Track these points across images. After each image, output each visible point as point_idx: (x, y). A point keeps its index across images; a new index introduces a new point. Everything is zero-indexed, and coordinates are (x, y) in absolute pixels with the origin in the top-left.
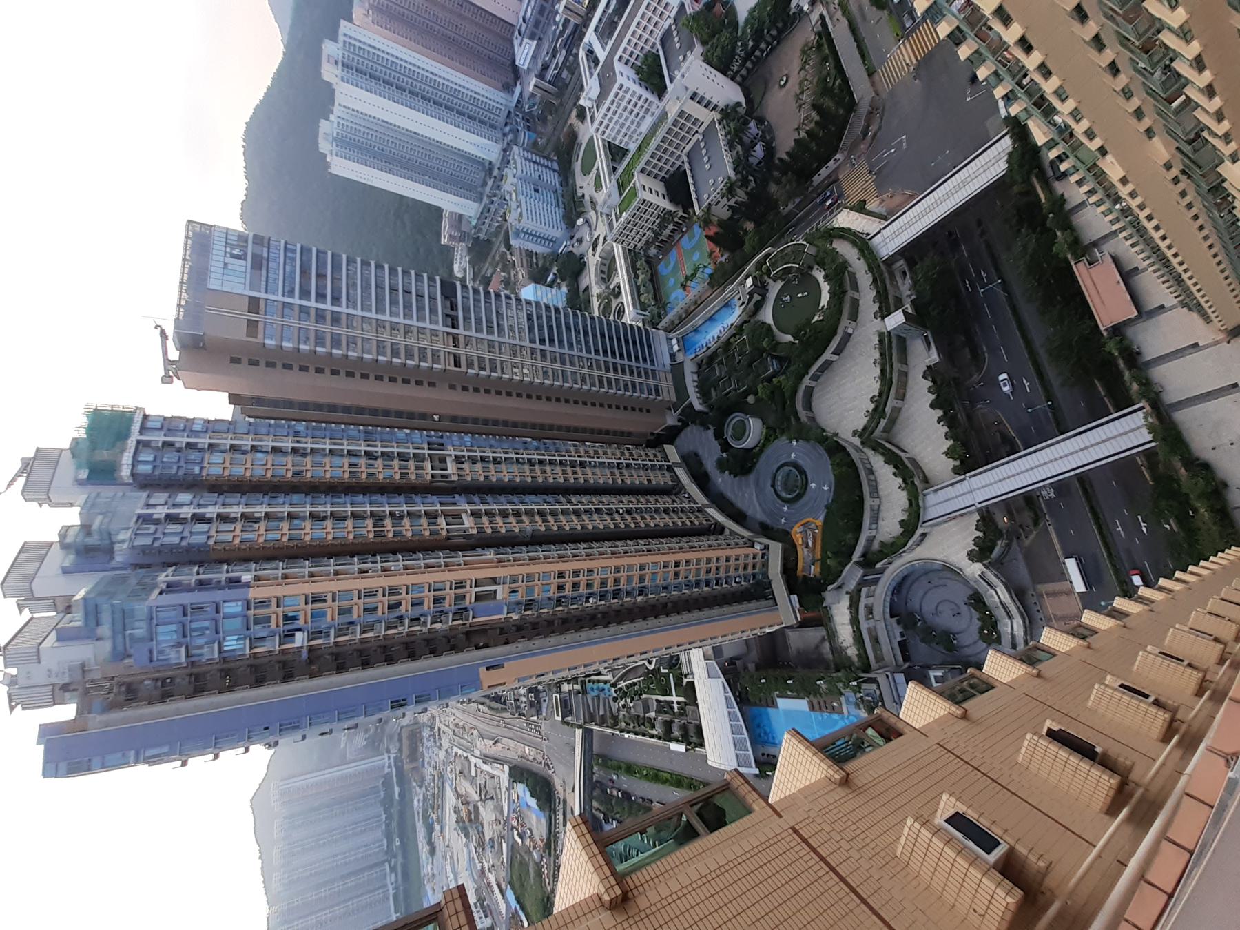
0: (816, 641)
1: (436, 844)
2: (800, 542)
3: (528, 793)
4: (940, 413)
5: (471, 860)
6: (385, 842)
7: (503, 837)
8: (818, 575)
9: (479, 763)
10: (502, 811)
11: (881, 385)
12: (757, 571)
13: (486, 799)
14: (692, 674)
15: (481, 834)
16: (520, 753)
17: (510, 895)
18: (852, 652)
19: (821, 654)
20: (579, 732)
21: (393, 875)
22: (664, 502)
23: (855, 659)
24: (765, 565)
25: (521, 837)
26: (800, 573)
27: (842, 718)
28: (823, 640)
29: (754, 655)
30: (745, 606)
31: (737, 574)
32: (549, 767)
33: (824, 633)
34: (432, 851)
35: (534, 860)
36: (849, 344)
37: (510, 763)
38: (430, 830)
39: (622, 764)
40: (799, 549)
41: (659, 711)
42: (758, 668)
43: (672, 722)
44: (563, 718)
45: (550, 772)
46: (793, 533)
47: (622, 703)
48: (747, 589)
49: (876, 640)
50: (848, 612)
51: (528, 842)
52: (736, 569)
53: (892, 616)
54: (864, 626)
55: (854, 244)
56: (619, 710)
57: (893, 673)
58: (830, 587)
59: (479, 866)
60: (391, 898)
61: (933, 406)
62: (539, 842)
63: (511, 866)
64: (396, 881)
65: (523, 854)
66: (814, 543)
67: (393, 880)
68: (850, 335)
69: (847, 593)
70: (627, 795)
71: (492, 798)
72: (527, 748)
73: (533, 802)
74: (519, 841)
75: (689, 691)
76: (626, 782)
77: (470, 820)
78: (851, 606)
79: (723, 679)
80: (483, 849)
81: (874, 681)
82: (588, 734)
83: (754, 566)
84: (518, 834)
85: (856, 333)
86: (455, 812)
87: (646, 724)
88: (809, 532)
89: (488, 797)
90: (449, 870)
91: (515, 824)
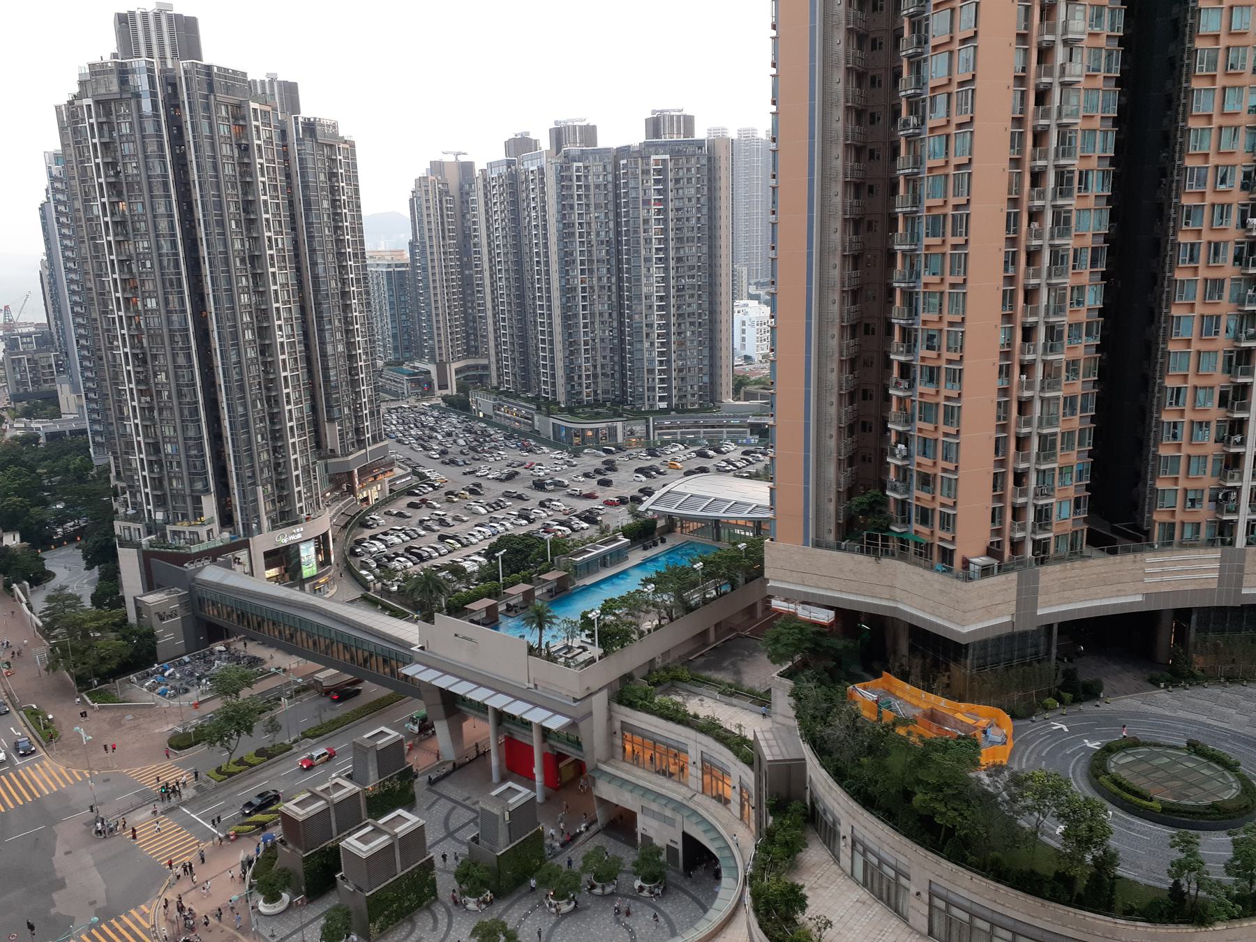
19: (724, 669)
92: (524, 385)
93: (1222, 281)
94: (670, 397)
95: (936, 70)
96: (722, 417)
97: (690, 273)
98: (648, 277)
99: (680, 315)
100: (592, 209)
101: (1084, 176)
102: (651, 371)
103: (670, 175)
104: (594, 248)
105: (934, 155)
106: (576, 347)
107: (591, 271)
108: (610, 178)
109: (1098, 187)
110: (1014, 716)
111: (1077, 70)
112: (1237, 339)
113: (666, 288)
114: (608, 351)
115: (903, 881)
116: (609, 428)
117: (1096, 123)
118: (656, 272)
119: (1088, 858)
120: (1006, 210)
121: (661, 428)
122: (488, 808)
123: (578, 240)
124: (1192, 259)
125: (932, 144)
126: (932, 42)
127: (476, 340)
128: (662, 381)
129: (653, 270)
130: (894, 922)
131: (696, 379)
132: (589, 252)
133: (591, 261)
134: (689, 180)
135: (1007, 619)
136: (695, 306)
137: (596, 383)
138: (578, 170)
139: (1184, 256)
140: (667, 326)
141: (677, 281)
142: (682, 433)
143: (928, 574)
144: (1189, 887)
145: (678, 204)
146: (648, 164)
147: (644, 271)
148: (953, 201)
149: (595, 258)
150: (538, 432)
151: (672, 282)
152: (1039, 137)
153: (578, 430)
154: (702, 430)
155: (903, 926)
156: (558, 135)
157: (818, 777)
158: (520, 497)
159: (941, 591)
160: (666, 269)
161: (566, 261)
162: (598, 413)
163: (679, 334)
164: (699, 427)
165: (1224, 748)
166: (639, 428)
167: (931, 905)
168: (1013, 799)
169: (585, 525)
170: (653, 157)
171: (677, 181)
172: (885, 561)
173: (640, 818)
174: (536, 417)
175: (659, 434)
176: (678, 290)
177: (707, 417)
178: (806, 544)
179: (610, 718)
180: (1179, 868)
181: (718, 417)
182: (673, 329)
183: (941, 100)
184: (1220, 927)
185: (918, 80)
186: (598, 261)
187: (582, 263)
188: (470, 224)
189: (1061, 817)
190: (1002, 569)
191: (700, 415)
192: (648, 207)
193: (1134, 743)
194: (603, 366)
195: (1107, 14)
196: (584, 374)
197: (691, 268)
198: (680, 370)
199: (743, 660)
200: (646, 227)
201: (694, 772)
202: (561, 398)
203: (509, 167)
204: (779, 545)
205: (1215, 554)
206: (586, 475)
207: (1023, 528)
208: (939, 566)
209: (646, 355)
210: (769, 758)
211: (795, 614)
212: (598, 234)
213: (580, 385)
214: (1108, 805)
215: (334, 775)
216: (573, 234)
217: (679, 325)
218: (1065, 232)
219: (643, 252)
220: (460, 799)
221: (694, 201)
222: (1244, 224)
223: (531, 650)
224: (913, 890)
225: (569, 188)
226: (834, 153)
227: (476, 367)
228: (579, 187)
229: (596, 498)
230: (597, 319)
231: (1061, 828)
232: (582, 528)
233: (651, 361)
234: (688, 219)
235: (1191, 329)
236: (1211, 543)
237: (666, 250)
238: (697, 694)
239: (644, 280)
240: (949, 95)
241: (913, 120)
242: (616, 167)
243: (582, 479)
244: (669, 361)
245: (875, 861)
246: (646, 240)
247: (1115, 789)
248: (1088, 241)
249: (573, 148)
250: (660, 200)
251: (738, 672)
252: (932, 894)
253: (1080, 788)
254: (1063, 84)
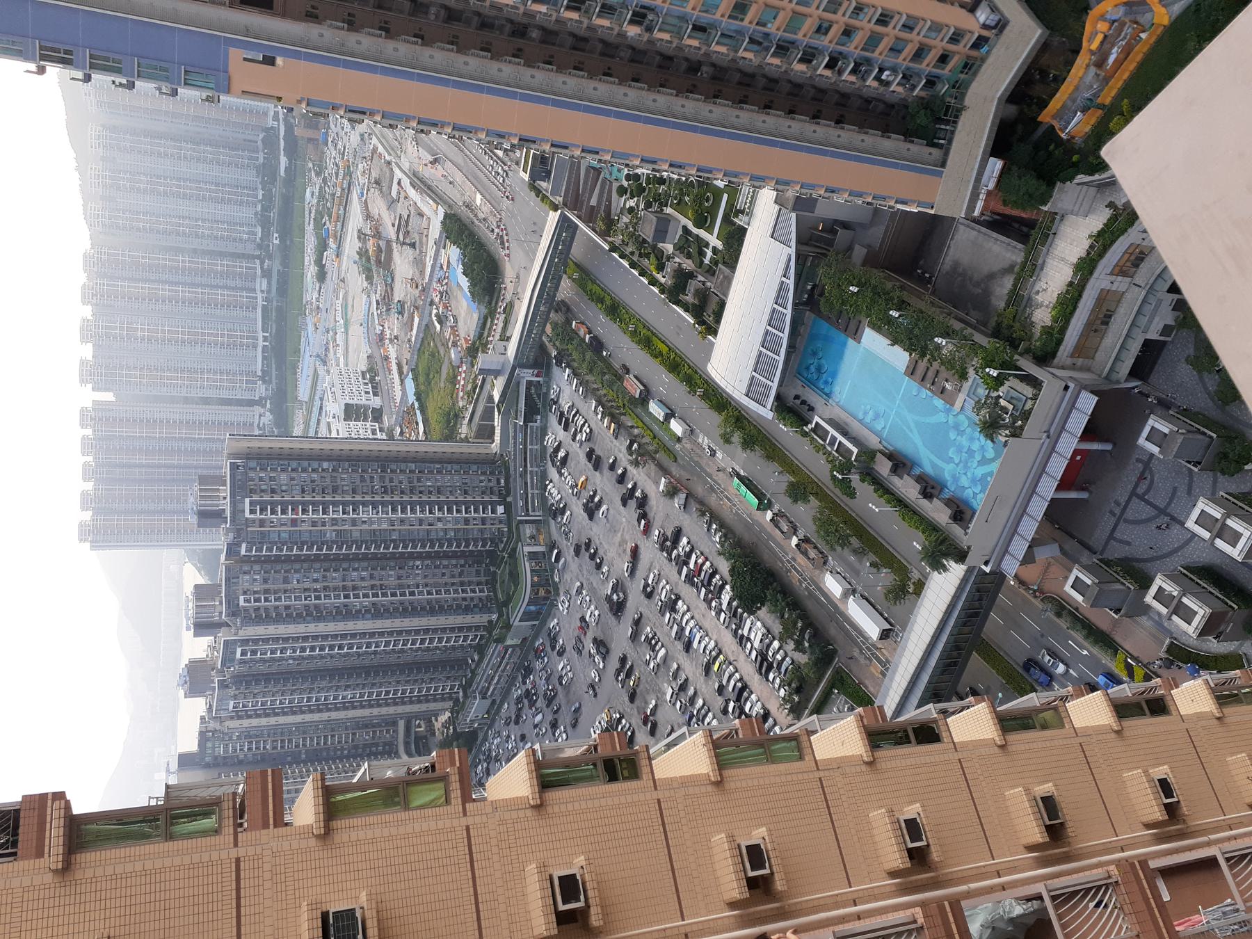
0: (997, 266)
1: (328, 268)
2: (1094, 46)
3: (460, 269)
5: (369, 314)
6: (259, 230)
7: (417, 308)
8: (1078, 140)
9: (406, 182)
10: (422, 272)
12: (946, 71)
13: (404, 243)
14: (750, 214)
15: (390, 287)
16: (468, 200)
17: (410, 384)
18: (1042, 316)
19: (987, 293)
20: (553, 217)
21: (265, 282)
23: (1037, 331)
24: (970, 67)
25: (440, 322)
26: (1046, 117)
27: (948, 411)
28: (1009, 270)
29: (876, 235)
30: (872, 139)
31: (891, 61)
32: (502, 243)
33: (1018, 257)
34: (322, 276)
35: (450, 358)
37: (450, 206)
38: (322, 247)
39: (607, 299)
40: (1082, 60)
41: (680, 248)
42: (871, 260)
43: (691, 275)
44: (533, 177)
45: (503, 253)
46: (1094, 13)
47: (632, 203)
48: (904, 105)
49: (1103, 317)
50: (1086, 244)
51: (447, 333)
52: (895, 50)
54: (1100, 280)
56: (621, 212)
57: (1083, 387)
58: (1081, 178)
59: (379, 328)
60: (259, 311)
62: (463, 341)
63: (420, 351)
64: (269, 292)
65: (439, 344)
66: (1119, 63)
67: (264, 287)
69: (1111, 205)
70: (597, 345)
71: (413, 245)
72: (479, 197)
73: (464, 282)
74: (438, 327)
75: (735, 238)
76: (605, 327)
77: (378, 262)
78: (1100, 234)
79: (792, 251)
80: (388, 310)
81: (1035, 383)
82: (565, 226)
83: (944, 59)
84: (437, 315)
86: (359, 238)
87: (652, 256)
88: (1128, 30)
89: (407, 241)
90: (339, 314)
91: (437, 300)
92: (460, 667)
94: (491, 503)
96: (515, 450)
97: (368, 481)
98: (372, 523)
99: (412, 492)
100: (289, 587)
102: (467, 521)
103: (267, 498)
104: (331, 585)
106: (434, 602)
107: (354, 588)
108: (257, 567)
113: (384, 504)
114: (437, 570)
116: (530, 559)
118: (366, 514)
121: (527, 510)
122: (1175, 449)
123: (323, 601)
127: (377, 745)
128: (476, 511)
129: (364, 517)
131: (473, 477)
132: (335, 589)
133: (344, 588)
134: (271, 479)
136: (402, 477)
137: (470, 583)
138: (248, 601)
140: (422, 504)
141: (376, 494)
142: (532, 489)
143: (990, 60)
145: (298, 490)
146: (254, 521)
147: (365, 527)
149: (341, 584)
150: (524, 640)
151: (377, 498)
153: (532, 590)
154: (529, 469)
156: (202, 627)
158: (637, 623)
159: (1007, 48)
160: (364, 504)
161: (346, 613)
162: (511, 574)
163: (430, 493)
164: (525, 471)
166: (528, 530)
169: (685, 540)
170: (247, 514)
171: (273, 491)
172: (967, 102)
173: (1148, 337)
174: (509, 642)
175: (534, 511)
176: (385, 492)
177: (515, 465)
178: (940, 174)
179: (1063, 368)
181: (515, 454)
182: (425, 498)
186: (344, 581)
187: (346, 597)
188: (250, 755)
191: (512, 469)
192: (299, 522)
194: (453, 576)
196: (461, 595)
197: (363, 479)
198: (466, 492)
199: (971, 279)
200: (320, 524)
201: (1121, 283)
202: (481, 619)
203: (227, 686)
204: (937, 200)
206: (599, 566)
208: (984, 50)
209: (450, 526)
211: (989, 193)
212: (316, 581)
213: (472, 599)
215: (1085, 652)
216: (316, 607)
217: (420, 492)
219: (346, 527)
220: (1113, 520)
221: (294, 475)
223: (1013, 435)
225: (266, 609)
226: (650, 103)
227: (407, 744)
228: (266, 600)
229: (636, 546)
230: (404, 582)
232: (688, 543)
233: (457, 521)
234: (313, 481)
237: (345, 504)
238: (1030, 298)
239: (375, 527)
242: (247, 560)
243: (605, 569)
244: (457, 503)
246: (333, 525)
249: (220, 610)
250: (292, 510)
251: (991, 276)
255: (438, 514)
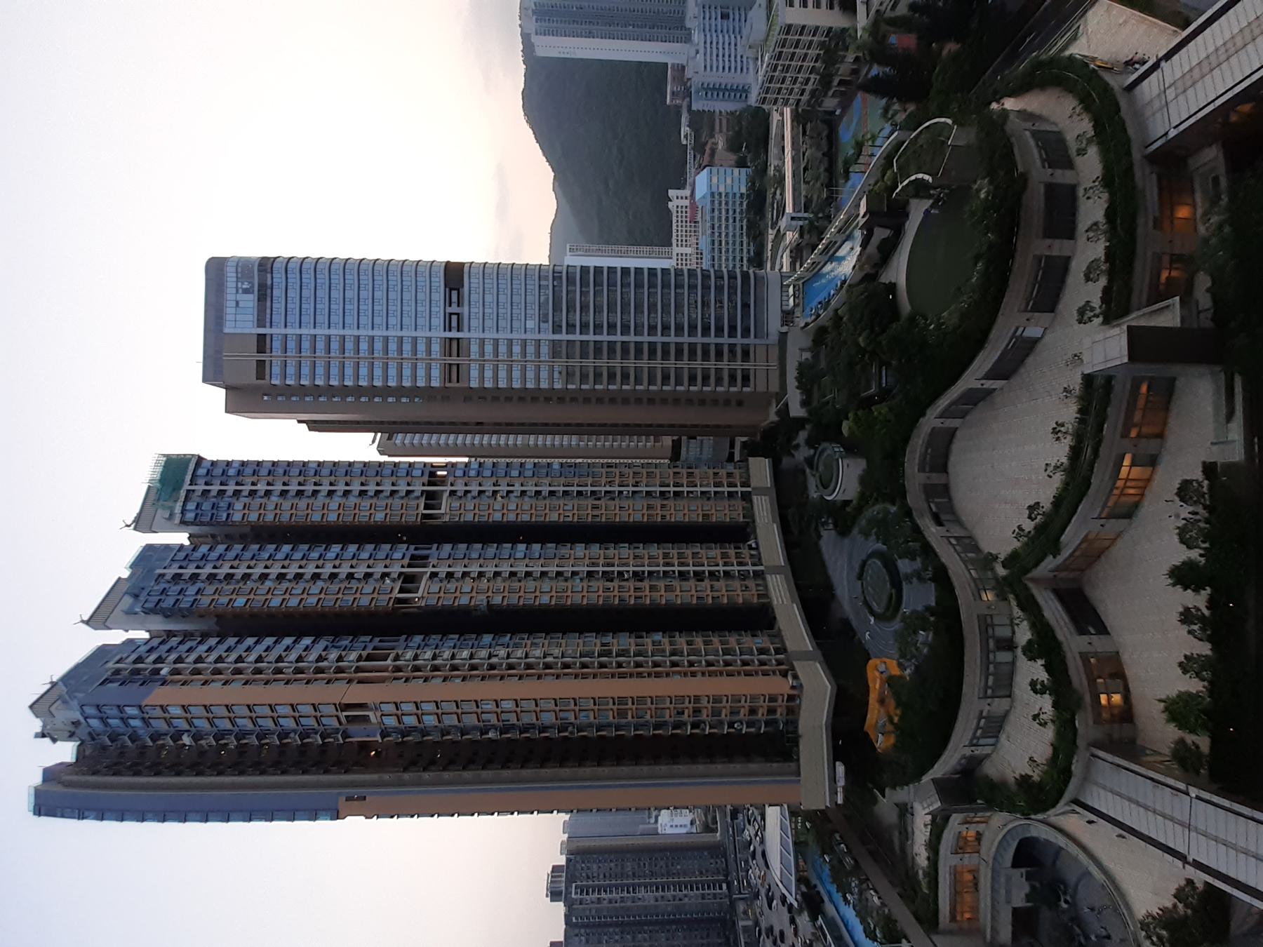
4: (1198, 600)
11: (1066, 484)
22: (710, 556)
24: (793, 712)
36: (1030, 360)
53: (1015, 864)
55: (1086, 103)
61: (1183, 576)
68: (1035, 342)
85: (1047, 339)
93: (650, 585)
95: (548, 718)
101: (603, 645)
105: (587, 717)
109: (609, 639)
110: (870, 659)
111: (557, 652)
112: (674, 578)
115: (984, 714)
117: (581, 641)
119: (932, 619)
120: (617, 679)
124: (641, 598)
125: (583, 719)
126: (534, 721)
130: (1012, 717)
135: (818, 665)
139: (639, 601)
143: (803, 707)
144: (929, 574)
148: (611, 706)
152: (584, 666)
155: (1012, 712)
157: (941, 769)
165: (857, 566)
167: (992, 697)
168: (913, 657)
172: (801, 730)
180: (920, 579)
183: (562, 715)
184: (943, 560)
185: (551, 727)
189: (915, 632)
190: (793, 669)
193: (866, 603)
195: (536, 641)
205: (768, 577)
207: (770, 660)
208: (798, 702)
210: (939, 804)
214: (901, 612)
218: (628, 651)
222: (627, 580)
224: (988, 708)
231: (921, 632)
235: (671, 596)
236: (764, 579)
240: (560, 711)
241: (570, 729)
245: (979, 732)
247: (891, 609)
248: (632, 641)
252: (986, 697)
253: (897, 625)
254: (562, 657)
255: (685, 892)
